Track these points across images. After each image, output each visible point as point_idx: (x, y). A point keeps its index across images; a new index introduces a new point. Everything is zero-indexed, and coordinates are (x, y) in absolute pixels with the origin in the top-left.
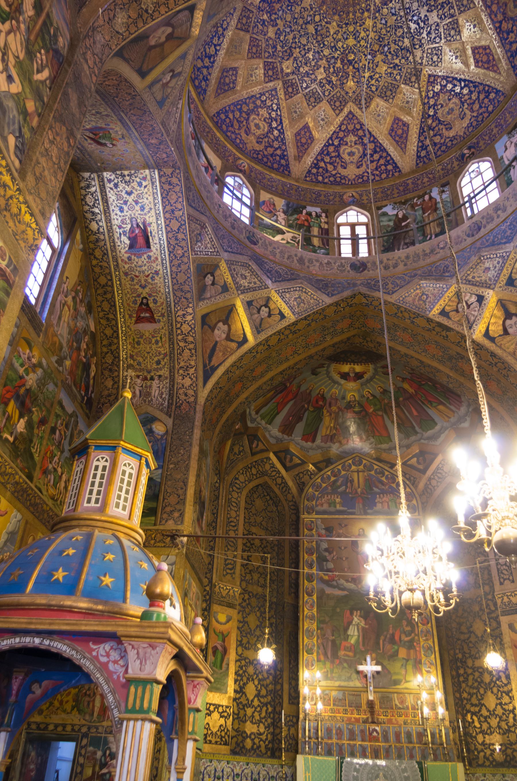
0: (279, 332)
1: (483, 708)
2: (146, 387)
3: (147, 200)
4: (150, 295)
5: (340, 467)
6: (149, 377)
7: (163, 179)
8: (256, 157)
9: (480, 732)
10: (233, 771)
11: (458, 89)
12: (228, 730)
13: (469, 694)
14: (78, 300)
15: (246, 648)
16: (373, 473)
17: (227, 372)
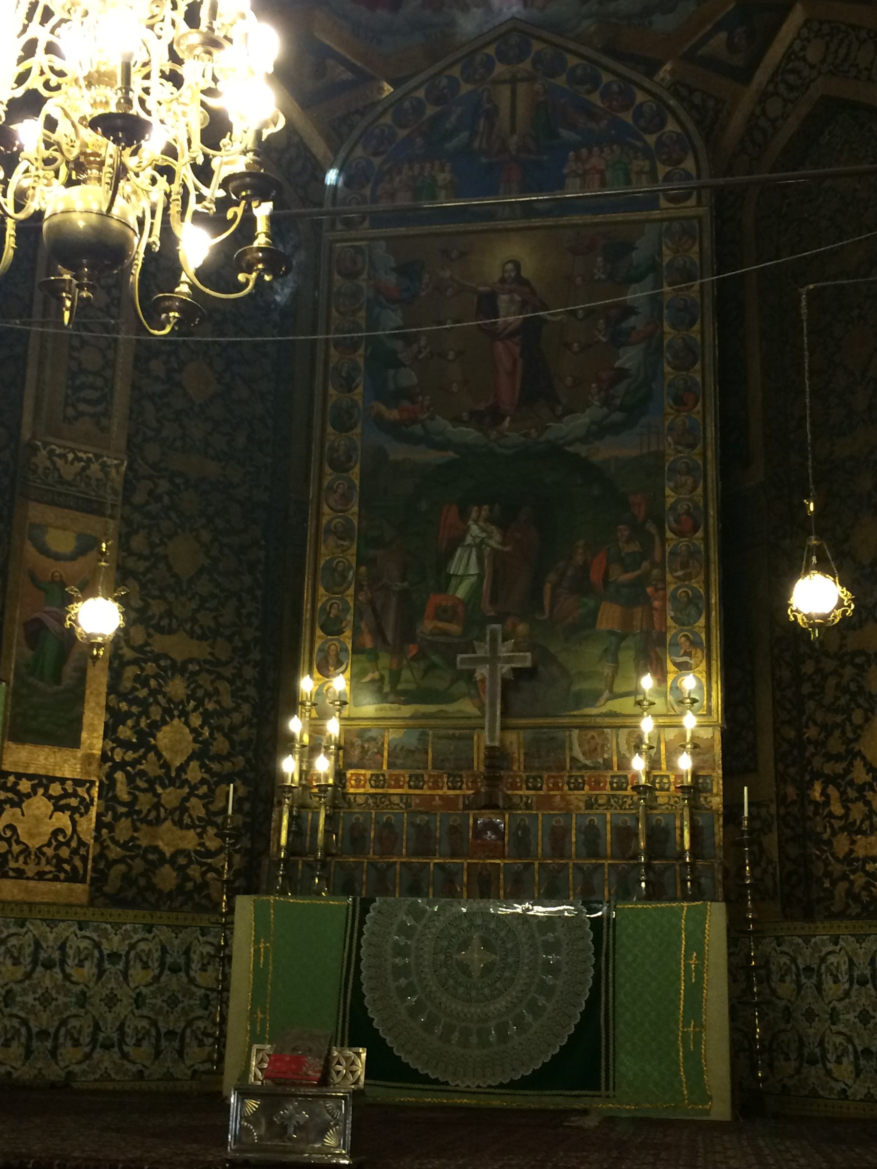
1: (858, 763)
5: (456, 71)
9: (842, 829)
10: (97, 945)
12: (81, 843)
13: (824, 727)
15: (161, 630)
16: (561, 81)
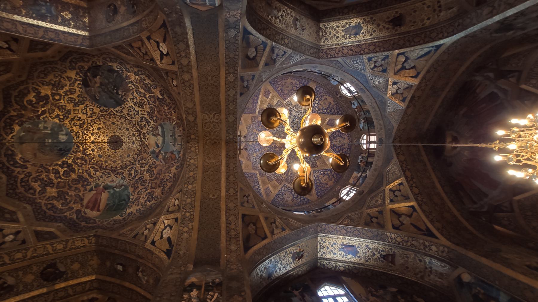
0: (411, 187)
2: (436, 273)
3: (331, 241)
4: (379, 253)
6: (430, 269)
7: (323, 232)
8: (337, 182)
11: (317, 102)
14: (375, 293)
17: (432, 222)
